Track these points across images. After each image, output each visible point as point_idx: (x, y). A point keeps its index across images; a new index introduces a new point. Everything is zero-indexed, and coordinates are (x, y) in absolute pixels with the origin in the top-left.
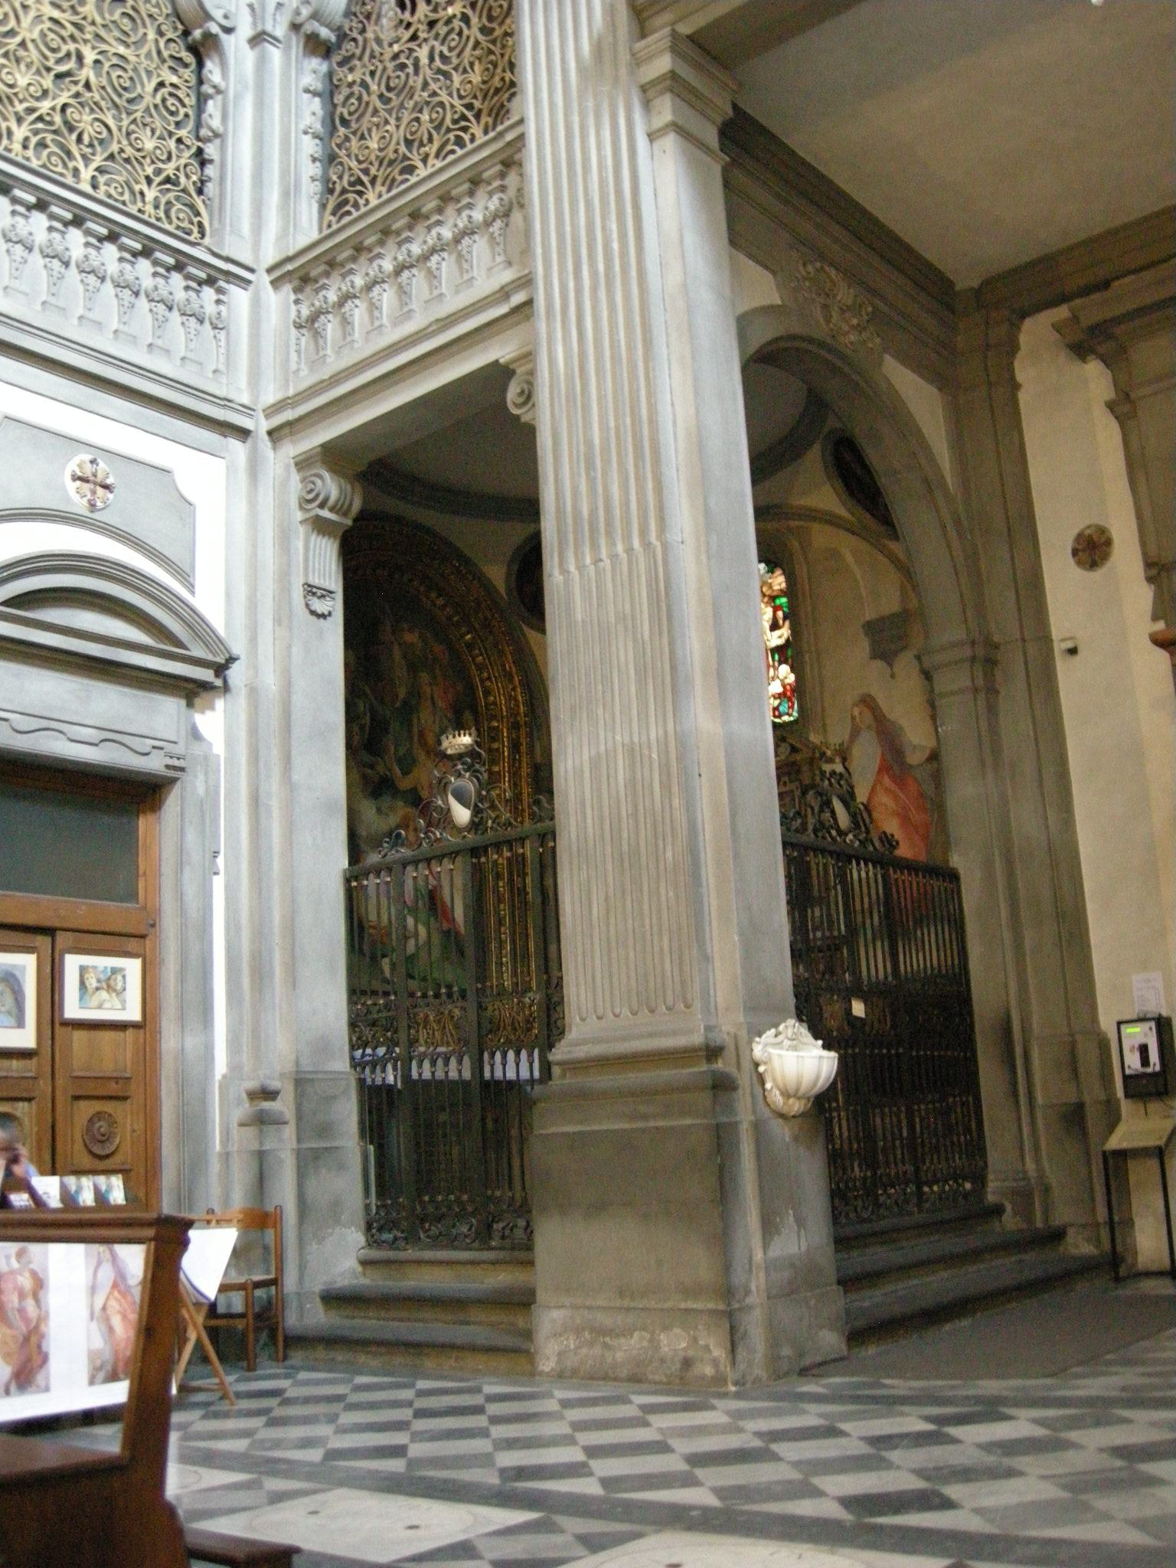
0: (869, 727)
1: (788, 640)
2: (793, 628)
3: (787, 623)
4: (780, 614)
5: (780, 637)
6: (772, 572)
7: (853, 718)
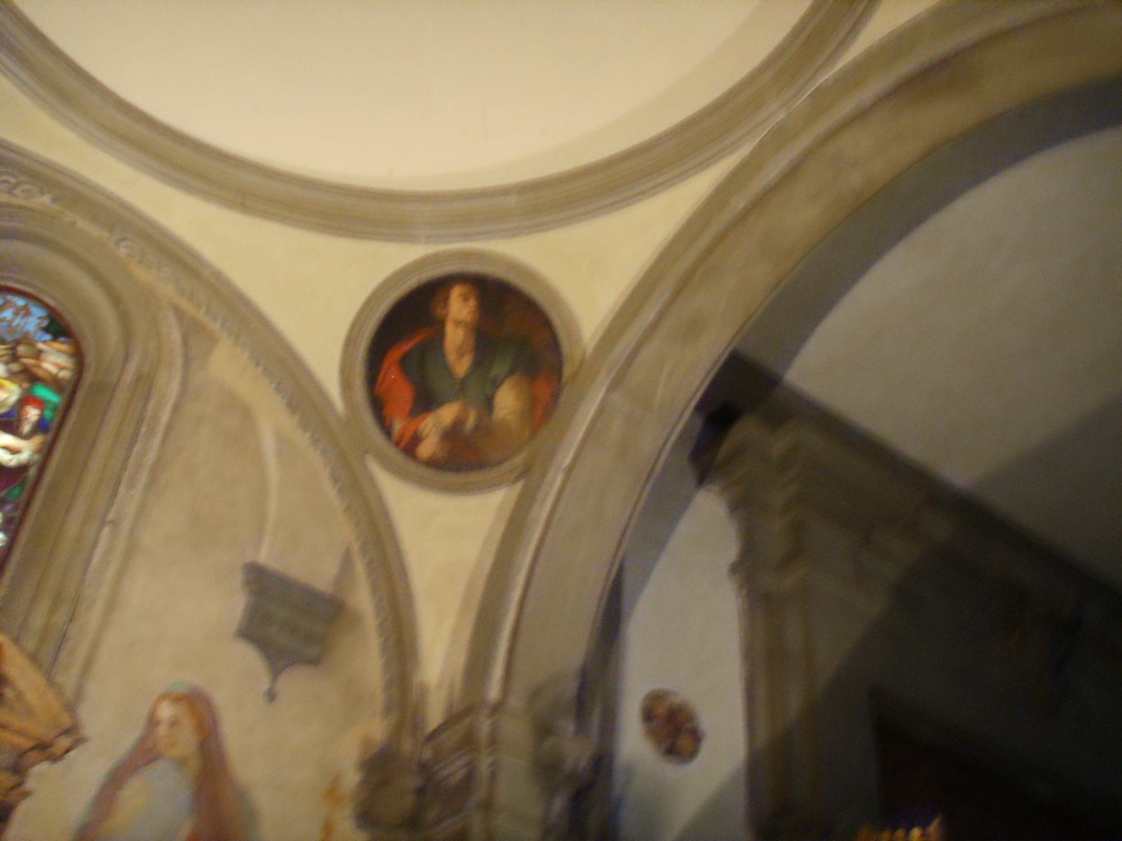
0: (181, 762)
1: (22, 469)
2: (46, 452)
3: (38, 440)
4: (33, 413)
5: (6, 448)
6: (55, 338)
7: (152, 722)
